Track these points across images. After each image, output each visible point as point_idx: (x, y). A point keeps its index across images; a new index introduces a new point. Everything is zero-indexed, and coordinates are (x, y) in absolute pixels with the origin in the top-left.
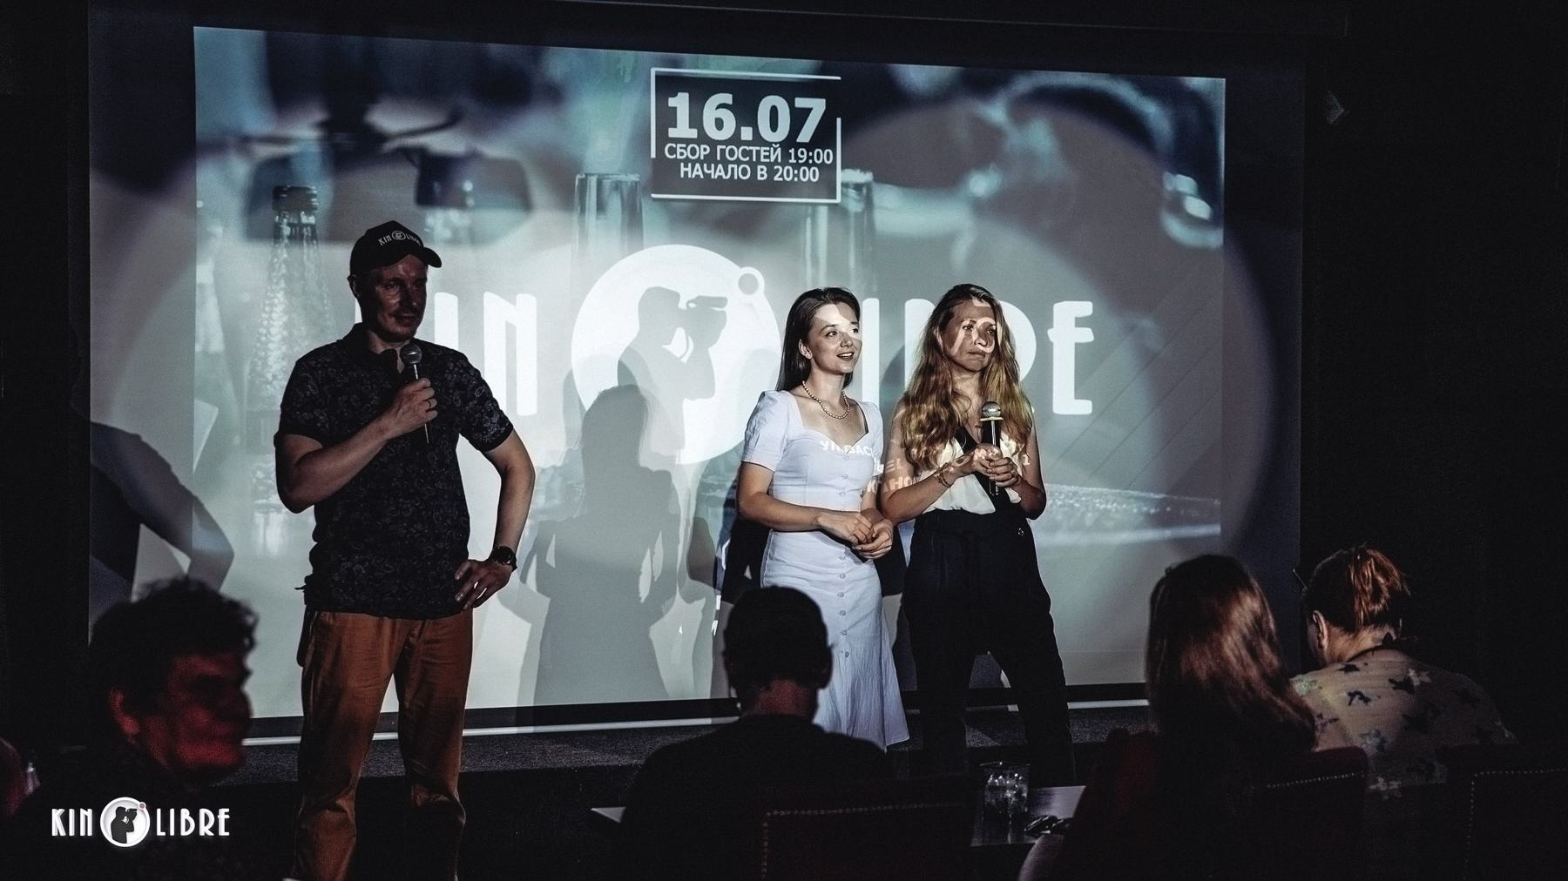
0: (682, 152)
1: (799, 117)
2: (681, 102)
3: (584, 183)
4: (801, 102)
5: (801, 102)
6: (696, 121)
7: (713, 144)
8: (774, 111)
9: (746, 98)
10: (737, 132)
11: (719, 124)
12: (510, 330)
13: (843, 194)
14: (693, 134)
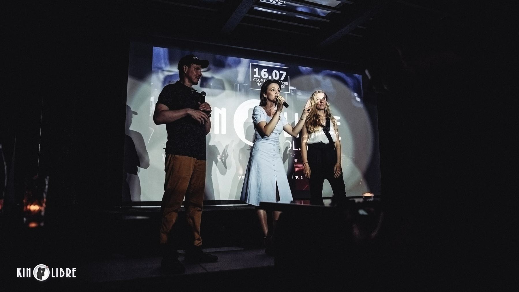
0: (257, 80)
1: (281, 75)
2: (257, 70)
3: (236, 85)
4: (281, 72)
5: (281, 72)
6: (260, 74)
7: (263, 79)
8: (276, 73)
9: (270, 70)
10: (268, 77)
11: (265, 75)
12: (220, 115)
13: (291, 92)
14: (259, 77)
